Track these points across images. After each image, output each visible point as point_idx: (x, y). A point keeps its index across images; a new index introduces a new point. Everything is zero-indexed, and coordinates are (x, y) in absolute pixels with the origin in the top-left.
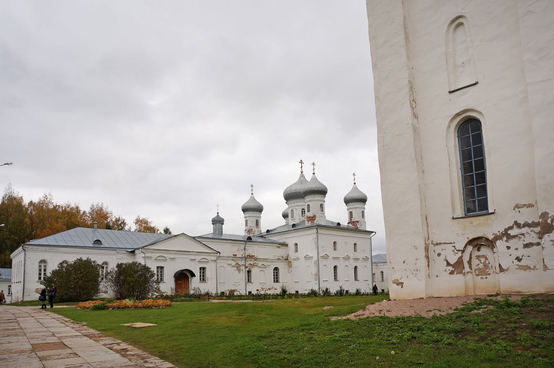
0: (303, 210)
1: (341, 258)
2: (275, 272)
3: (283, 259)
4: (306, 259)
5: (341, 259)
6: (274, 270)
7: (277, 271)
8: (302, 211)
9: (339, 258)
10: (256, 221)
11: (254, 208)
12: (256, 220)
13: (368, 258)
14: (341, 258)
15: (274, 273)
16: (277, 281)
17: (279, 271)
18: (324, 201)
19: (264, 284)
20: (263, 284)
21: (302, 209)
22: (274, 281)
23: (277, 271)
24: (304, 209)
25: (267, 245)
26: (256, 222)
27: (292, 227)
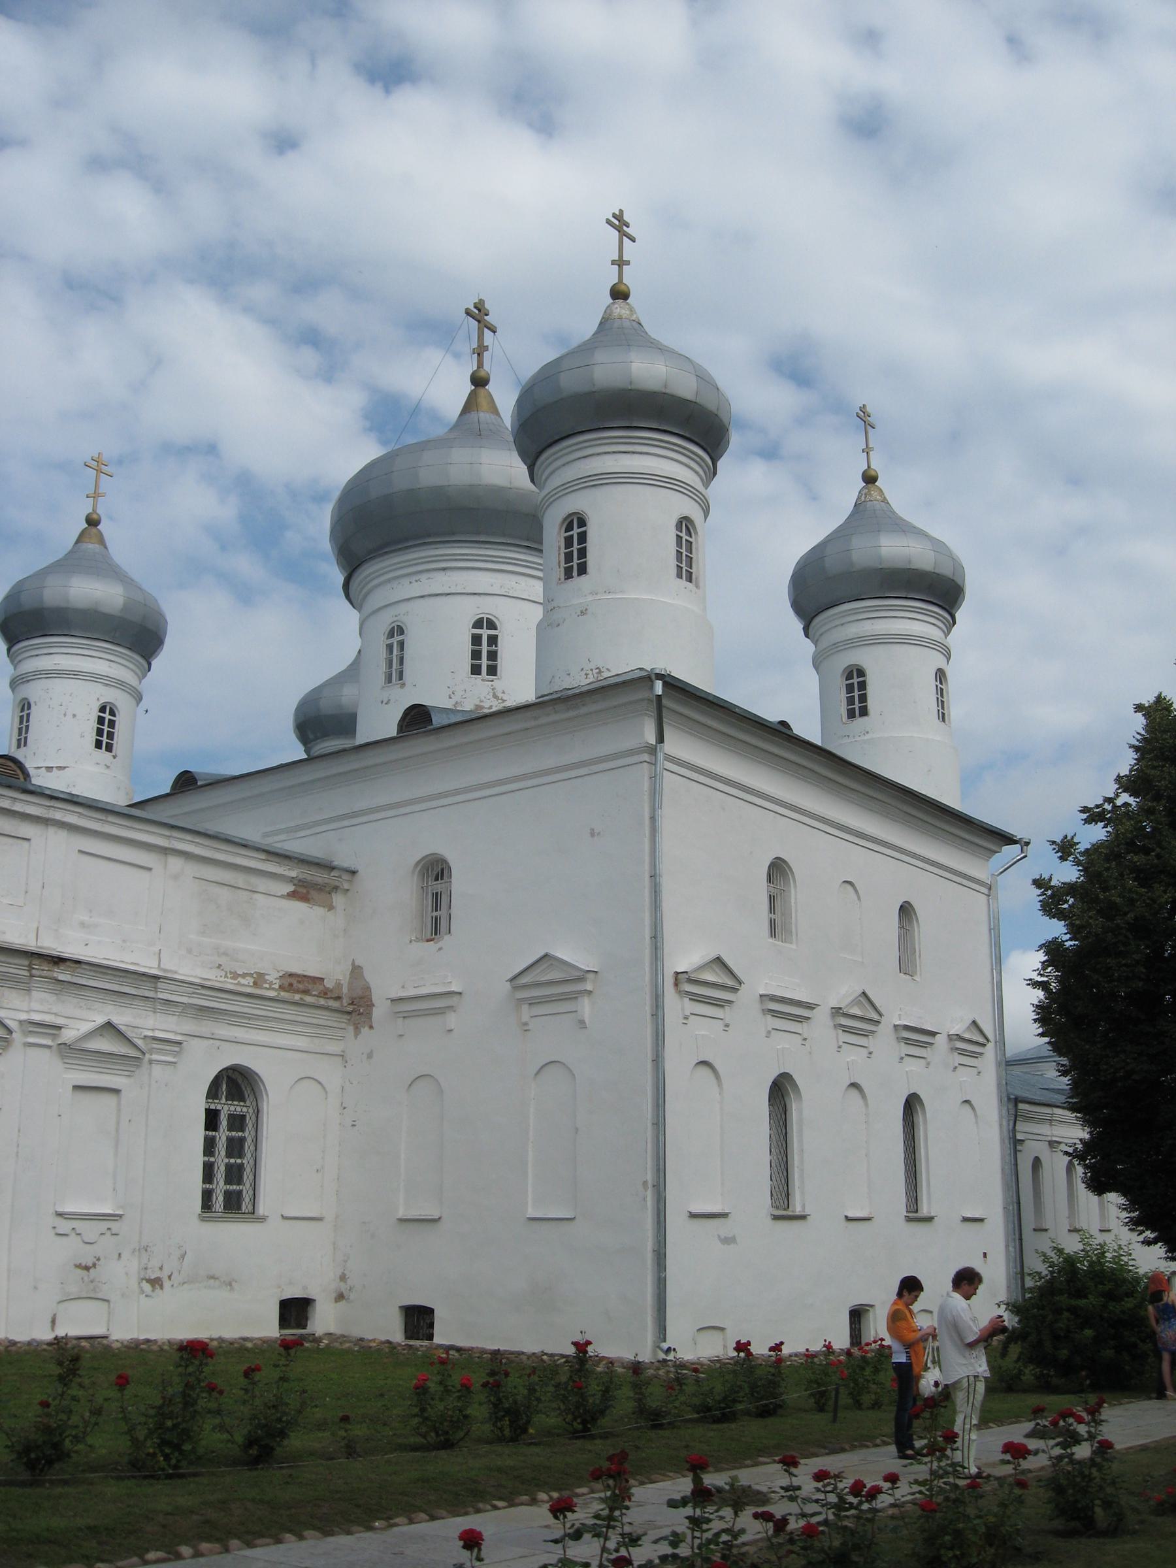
0: (485, 633)
1: (821, 1017)
2: (226, 1108)
5: (821, 1025)
8: (476, 640)
9: (810, 1007)
10: (95, 714)
11: (96, 611)
12: (103, 709)
14: (821, 1017)
16: (233, 1203)
17: (258, 1112)
19: (103, 1226)
20: (90, 1230)
21: (478, 624)
23: (237, 1108)
24: (492, 625)
25: (165, 851)
26: (101, 721)
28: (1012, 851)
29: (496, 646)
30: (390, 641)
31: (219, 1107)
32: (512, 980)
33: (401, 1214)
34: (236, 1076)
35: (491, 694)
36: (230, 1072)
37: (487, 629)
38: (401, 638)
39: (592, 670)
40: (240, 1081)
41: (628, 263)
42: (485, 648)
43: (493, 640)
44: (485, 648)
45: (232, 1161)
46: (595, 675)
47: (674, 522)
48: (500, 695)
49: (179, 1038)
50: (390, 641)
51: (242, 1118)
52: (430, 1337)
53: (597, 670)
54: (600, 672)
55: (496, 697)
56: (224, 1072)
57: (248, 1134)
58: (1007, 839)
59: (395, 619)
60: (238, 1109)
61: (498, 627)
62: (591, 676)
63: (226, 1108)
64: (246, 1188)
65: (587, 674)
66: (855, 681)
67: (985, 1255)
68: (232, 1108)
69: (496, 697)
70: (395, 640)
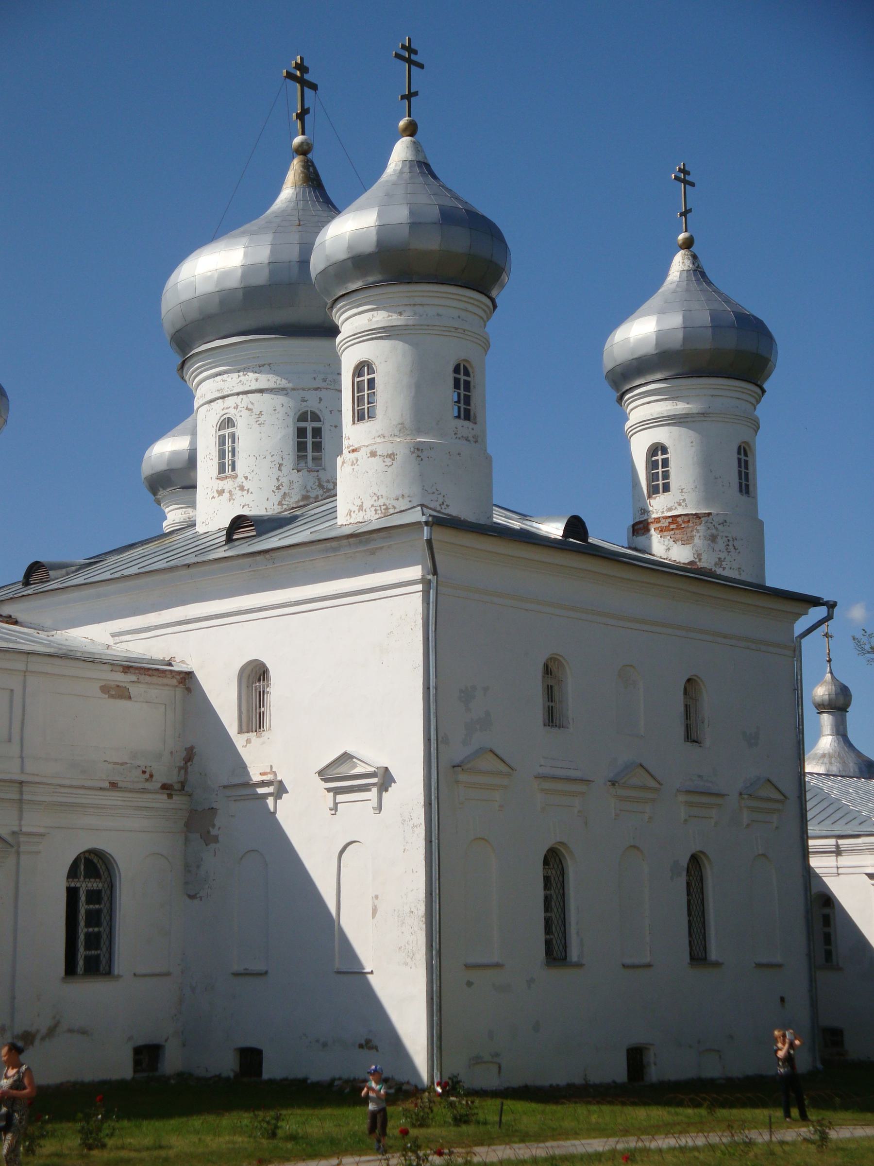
0: (309, 426)
2: (85, 886)
3: (148, 785)
4: (337, 791)
6: (73, 872)
7: (94, 885)
13: (778, 796)
15: (72, 894)
17: (112, 887)
18: (486, 346)
22: (70, 970)
23: (94, 885)
24: (316, 417)
27: (229, 539)
28: (819, 612)
29: (321, 438)
30: (221, 433)
31: (78, 885)
32: (320, 773)
33: (236, 968)
34: (92, 857)
35: (317, 484)
36: (87, 855)
37: (312, 421)
38: (231, 430)
39: (380, 506)
40: (95, 861)
41: (416, 94)
42: (309, 440)
43: (317, 432)
44: (309, 440)
45: (91, 930)
46: (383, 511)
47: (451, 368)
48: (325, 484)
49: (42, 830)
50: (221, 433)
51: (99, 892)
52: (259, 1073)
53: (385, 507)
54: (387, 509)
55: (321, 486)
56: (82, 856)
57: (103, 906)
58: (816, 602)
59: (225, 411)
60: (95, 885)
61: (322, 420)
62: (379, 512)
63: (84, 885)
64: (103, 952)
65: (376, 510)
66: (660, 457)
67: (782, 999)
68: (90, 885)
69: (321, 486)
70: (226, 432)
